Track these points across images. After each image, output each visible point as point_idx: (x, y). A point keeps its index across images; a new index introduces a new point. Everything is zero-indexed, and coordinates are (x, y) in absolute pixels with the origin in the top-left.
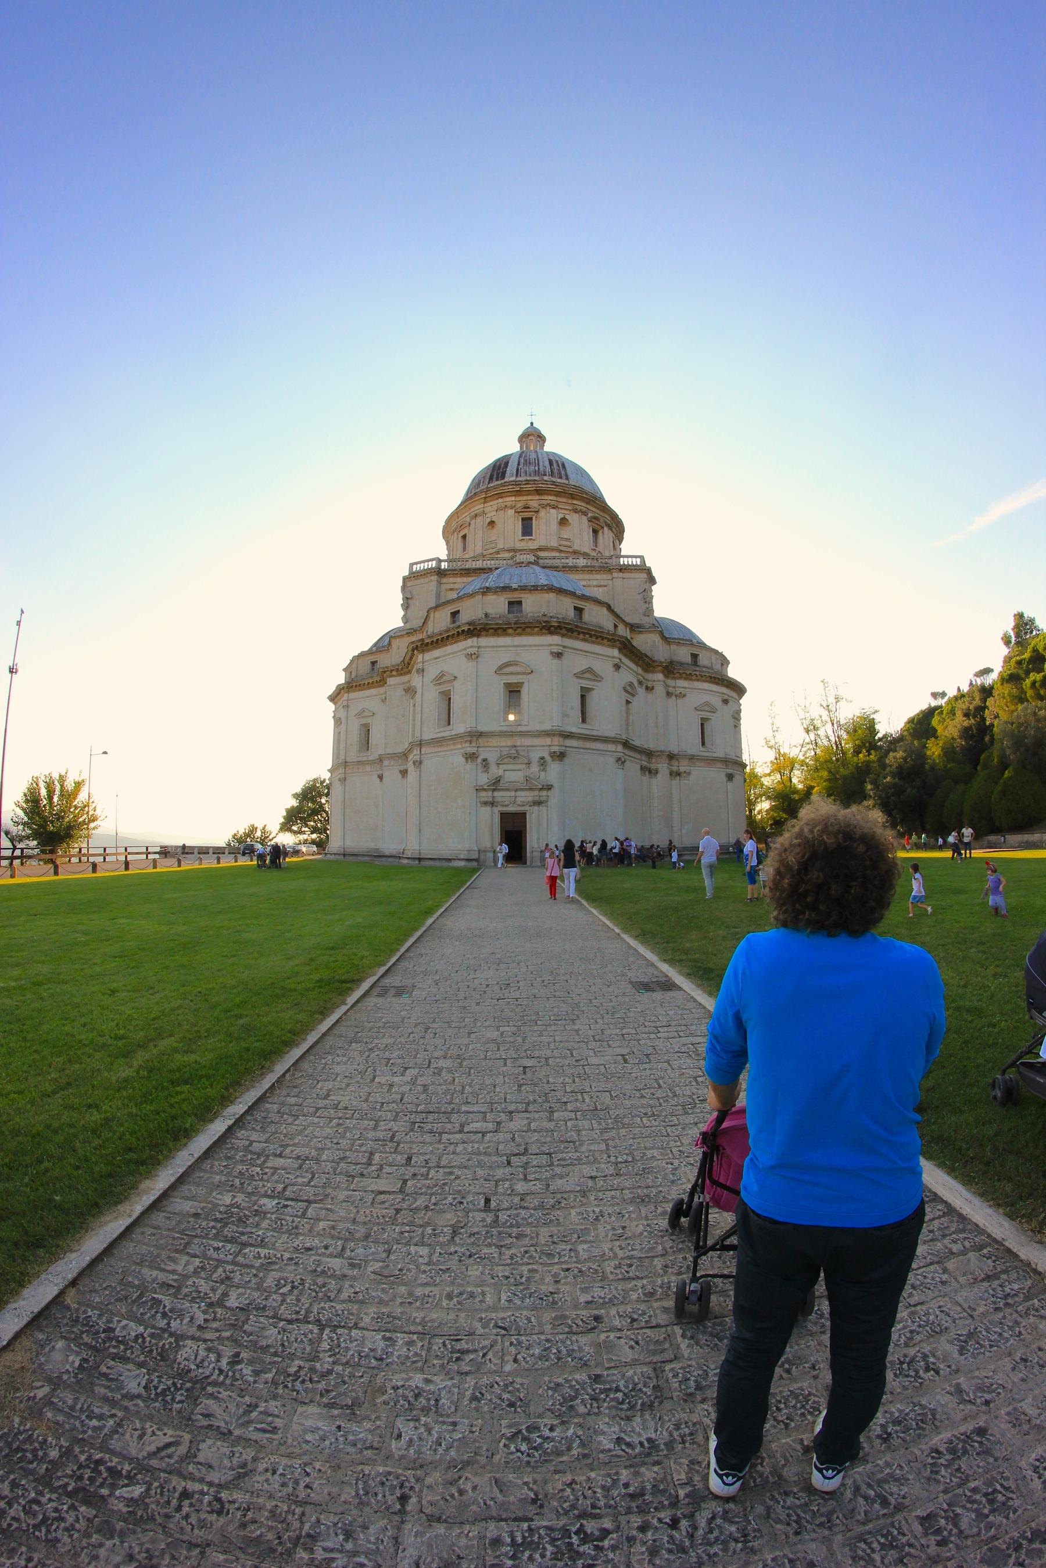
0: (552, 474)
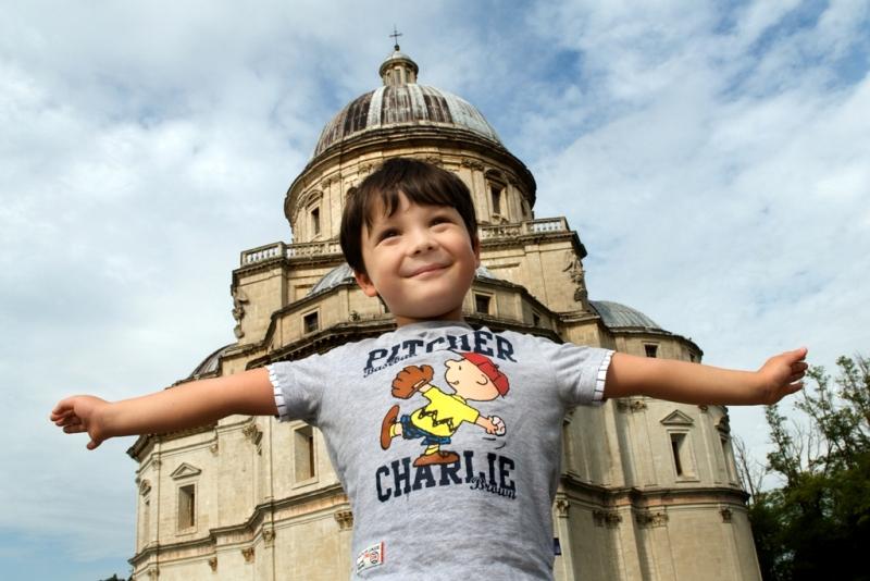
0: (430, 119)
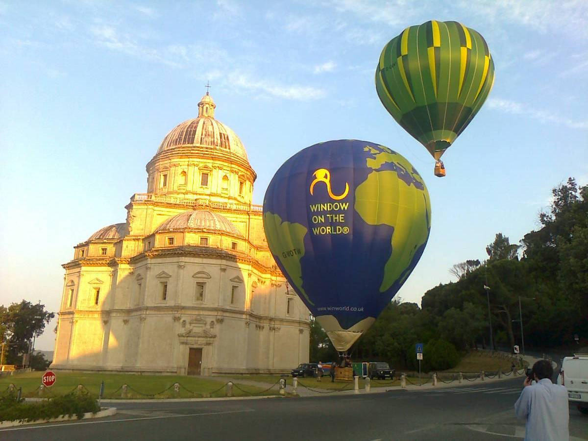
0: (221, 147)
